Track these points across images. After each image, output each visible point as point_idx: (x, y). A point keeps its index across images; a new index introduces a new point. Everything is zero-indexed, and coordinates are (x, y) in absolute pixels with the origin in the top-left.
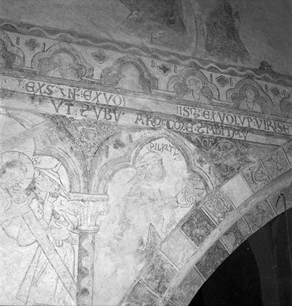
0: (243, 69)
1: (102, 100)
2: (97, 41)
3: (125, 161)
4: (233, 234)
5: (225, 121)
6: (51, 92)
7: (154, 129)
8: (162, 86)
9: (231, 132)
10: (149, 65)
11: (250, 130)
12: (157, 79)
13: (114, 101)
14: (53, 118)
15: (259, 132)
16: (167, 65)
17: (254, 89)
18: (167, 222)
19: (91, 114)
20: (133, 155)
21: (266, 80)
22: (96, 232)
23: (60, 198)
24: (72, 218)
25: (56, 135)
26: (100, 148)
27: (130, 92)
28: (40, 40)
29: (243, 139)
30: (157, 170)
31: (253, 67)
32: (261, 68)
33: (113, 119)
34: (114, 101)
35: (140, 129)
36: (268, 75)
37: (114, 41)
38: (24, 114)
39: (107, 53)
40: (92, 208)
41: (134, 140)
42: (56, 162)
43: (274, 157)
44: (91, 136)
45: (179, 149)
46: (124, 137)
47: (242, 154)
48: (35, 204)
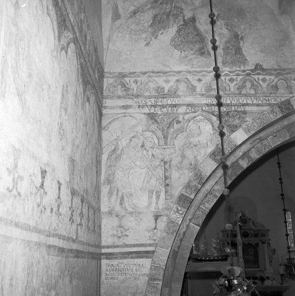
0: (244, 71)
1: (169, 102)
2: (165, 73)
3: (181, 130)
4: (247, 159)
5: (233, 102)
6: (146, 103)
7: (195, 112)
8: (198, 90)
9: (236, 107)
10: (191, 80)
11: (247, 105)
12: (196, 87)
13: (175, 102)
14: (148, 114)
15: (253, 105)
16: (200, 77)
17: (251, 81)
18: (203, 155)
19: (165, 110)
20: (186, 126)
21: (259, 74)
22: (171, 161)
23: (155, 148)
24: (160, 156)
25: (150, 122)
26: (170, 125)
27: (182, 96)
28: (139, 79)
29: (243, 110)
30: (198, 131)
31: (250, 68)
32: (255, 68)
33: (175, 111)
34: (175, 102)
35: (188, 113)
36: (259, 71)
37: (173, 72)
38: (136, 115)
39: (170, 78)
40: (168, 151)
41: (186, 119)
42: (151, 134)
43: (261, 117)
44: (165, 120)
45: (208, 120)
46: (181, 118)
47: (242, 118)
48: (145, 152)
